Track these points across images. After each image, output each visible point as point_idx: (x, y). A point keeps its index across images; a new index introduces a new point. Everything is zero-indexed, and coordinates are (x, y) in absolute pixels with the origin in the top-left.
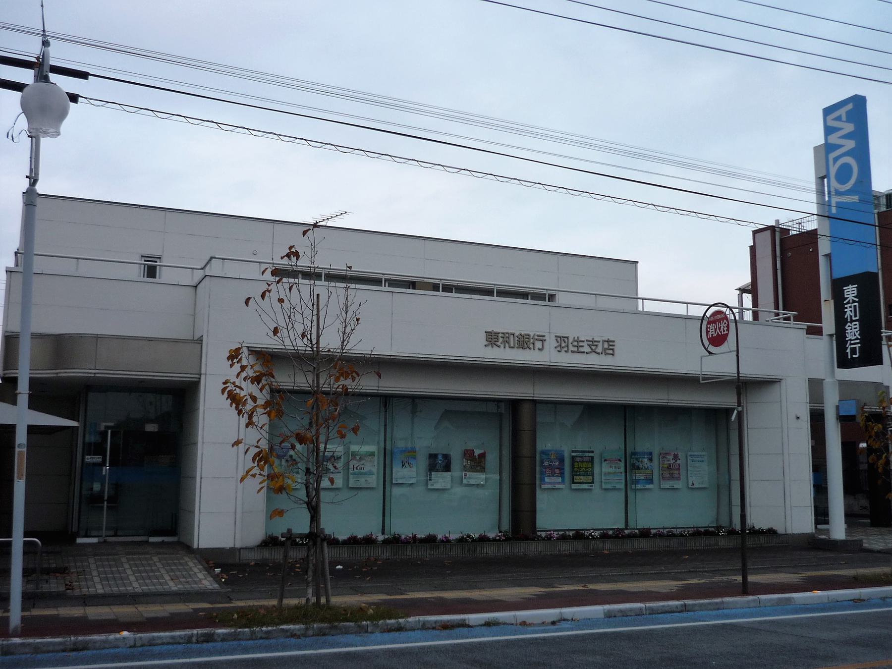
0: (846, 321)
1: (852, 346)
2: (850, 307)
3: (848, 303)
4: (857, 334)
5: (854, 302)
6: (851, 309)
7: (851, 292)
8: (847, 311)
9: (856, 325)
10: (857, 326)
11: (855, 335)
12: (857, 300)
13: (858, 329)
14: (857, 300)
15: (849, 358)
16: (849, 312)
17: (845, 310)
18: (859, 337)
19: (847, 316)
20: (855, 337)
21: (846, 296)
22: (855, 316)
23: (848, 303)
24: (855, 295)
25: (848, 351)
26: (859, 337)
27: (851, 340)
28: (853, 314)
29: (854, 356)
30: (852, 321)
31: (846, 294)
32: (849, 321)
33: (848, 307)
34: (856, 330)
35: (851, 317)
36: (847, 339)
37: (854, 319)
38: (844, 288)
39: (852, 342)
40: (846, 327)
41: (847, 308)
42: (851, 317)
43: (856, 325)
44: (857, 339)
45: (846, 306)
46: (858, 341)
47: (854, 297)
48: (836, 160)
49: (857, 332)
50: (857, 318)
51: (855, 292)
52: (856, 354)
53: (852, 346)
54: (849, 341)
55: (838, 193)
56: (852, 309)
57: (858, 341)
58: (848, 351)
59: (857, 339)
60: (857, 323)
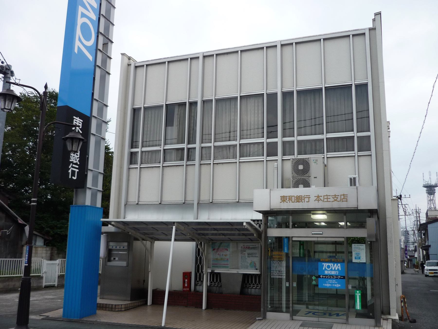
11: (76, 160)
13: (78, 157)
15: (70, 177)
18: (79, 163)
20: (76, 162)
25: (70, 171)
26: (79, 163)
27: (72, 162)
29: (73, 177)
34: (77, 156)
36: (70, 160)
38: (74, 117)
39: (74, 165)
44: (76, 164)
46: (77, 167)
49: (78, 158)
52: (75, 177)
54: (71, 164)
57: (77, 167)
58: (70, 171)
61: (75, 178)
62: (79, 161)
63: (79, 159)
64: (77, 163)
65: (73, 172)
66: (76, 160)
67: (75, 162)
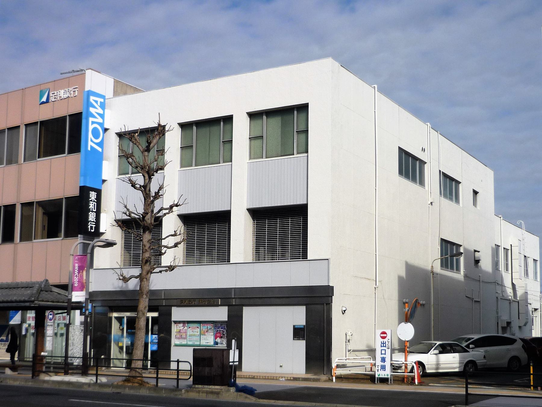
2: (92, 203)
3: (91, 201)
4: (94, 219)
6: (93, 205)
8: (90, 205)
9: (94, 214)
10: (95, 215)
11: (93, 219)
13: (95, 217)
14: (96, 201)
15: (90, 230)
17: (90, 204)
21: (91, 197)
22: (94, 209)
23: (91, 201)
24: (95, 198)
25: (89, 227)
26: (95, 221)
27: (90, 221)
28: (93, 208)
29: (92, 231)
30: (92, 211)
31: (91, 195)
32: (91, 210)
33: (91, 203)
34: (94, 217)
35: (92, 209)
36: (89, 220)
37: (94, 210)
38: (91, 192)
39: (92, 223)
40: (90, 213)
41: (91, 203)
42: (92, 209)
43: (94, 214)
44: (93, 222)
46: (94, 223)
49: (94, 218)
50: (95, 210)
51: (96, 196)
52: (93, 230)
54: (90, 222)
56: (93, 205)
57: (94, 223)
58: (89, 227)
59: (93, 222)
60: (95, 213)
61: (93, 231)
62: (95, 220)
63: (95, 218)
64: (94, 221)
65: (91, 228)
66: (93, 219)
67: (92, 221)
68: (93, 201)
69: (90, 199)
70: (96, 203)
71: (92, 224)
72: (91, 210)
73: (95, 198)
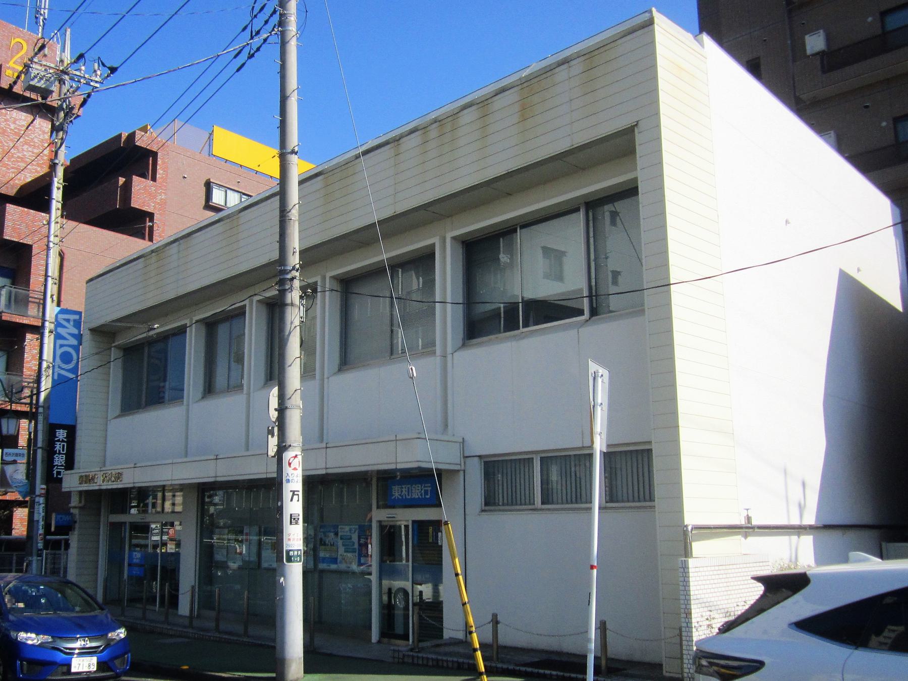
0: (55, 453)
1: (58, 470)
2: (60, 444)
3: (59, 441)
4: (63, 463)
5: (63, 441)
7: (61, 434)
9: (63, 456)
12: (65, 440)
13: (64, 459)
14: (65, 440)
16: (58, 447)
19: (57, 450)
23: (59, 441)
25: (55, 472)
27: (57, 465)
29: (59, 476)
30: (60, 453)
31: (57, 434)
32: (58, 452)
35: (59, 451)
40: (55, 456)
41: (57, 444)
42: (59, 451)
43: (63, 456)
44: (62, 466)
45: (56, 443)
46: (63, 468)
47: (65, 438)
48: (61, 346)
50: (65, 452)
53: (58, 470)
55: (59, 367)
57: (63, 468)
58: (55, 472)
59: (62, 466)
67: (60, 464)
68: (61, 440)
69: (56, 439)
70: (65, 444)
71: (59, 469)
72: (58, 452)
73: (65, 436)
